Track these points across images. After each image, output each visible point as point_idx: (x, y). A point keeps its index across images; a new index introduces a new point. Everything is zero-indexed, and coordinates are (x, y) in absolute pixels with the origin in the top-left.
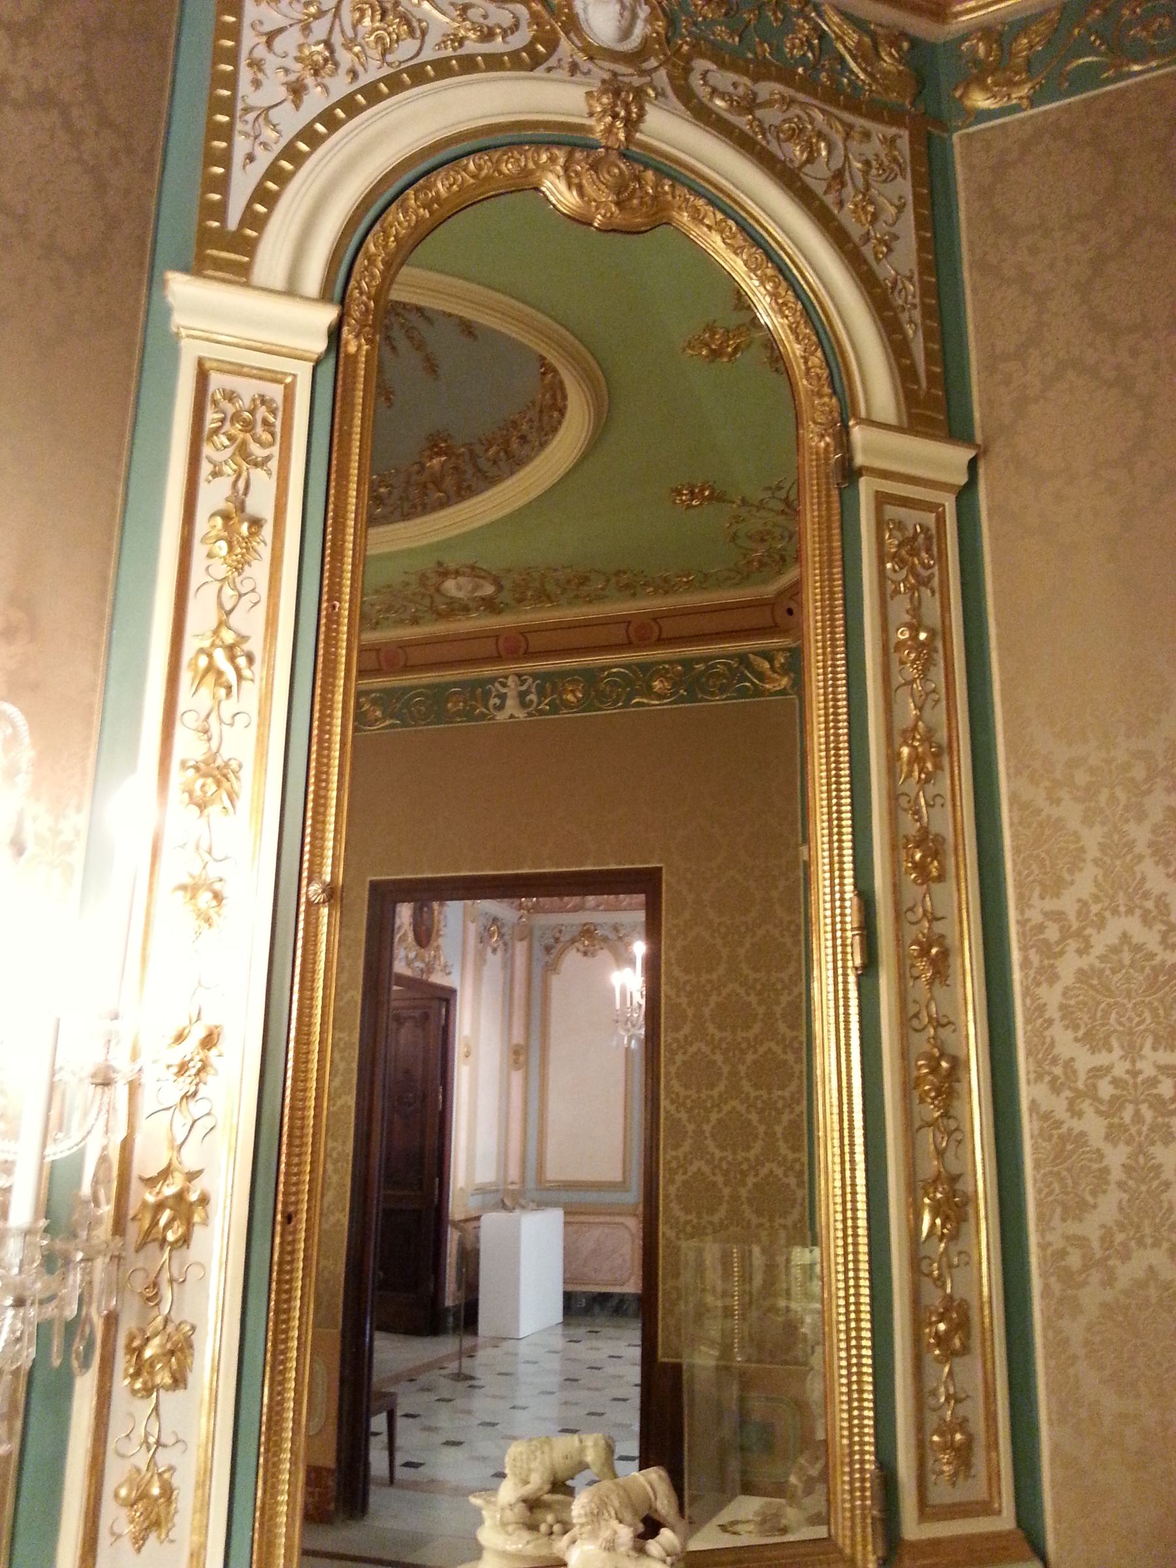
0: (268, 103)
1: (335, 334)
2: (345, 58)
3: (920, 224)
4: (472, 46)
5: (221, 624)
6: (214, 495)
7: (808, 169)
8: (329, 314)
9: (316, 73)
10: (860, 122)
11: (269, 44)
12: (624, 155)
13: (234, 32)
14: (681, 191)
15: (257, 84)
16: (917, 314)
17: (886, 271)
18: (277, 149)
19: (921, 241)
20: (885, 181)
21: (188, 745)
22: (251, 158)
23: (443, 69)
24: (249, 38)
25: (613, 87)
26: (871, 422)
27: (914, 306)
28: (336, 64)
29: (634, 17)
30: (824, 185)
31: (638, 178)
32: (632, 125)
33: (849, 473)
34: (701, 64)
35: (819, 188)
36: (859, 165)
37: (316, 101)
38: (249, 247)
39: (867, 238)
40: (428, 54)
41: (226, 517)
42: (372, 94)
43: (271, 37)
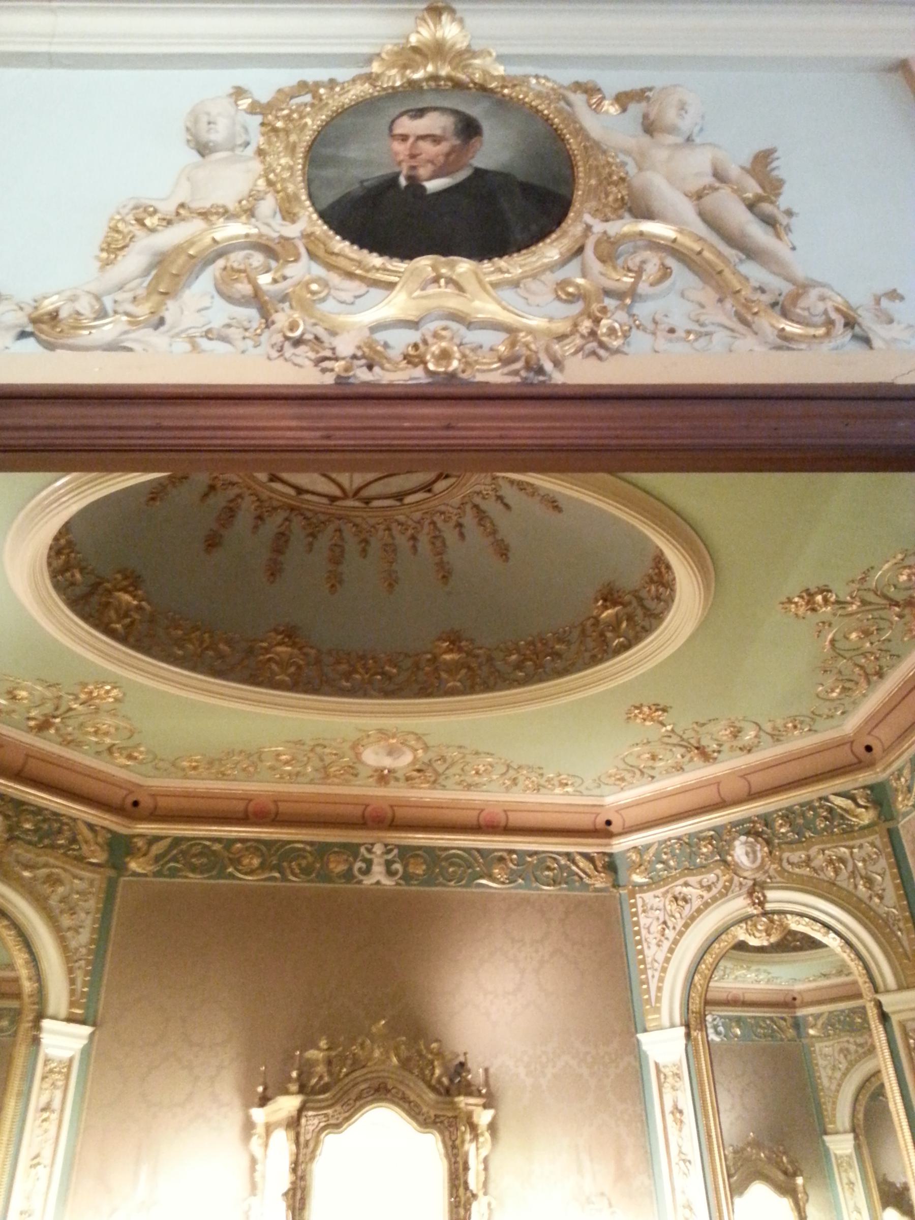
0: (653, 952)
1: (688, 1035)
2: (670, 924)
3: (894, 879)
4: (707, 895)
5: (681, 1152)
6: (668, 1107)
7: (838, 878)
8: (682, 1030)
9: (663, 935)
10: (857, 842)
11: (649, 932)
12: (765, 914)
13: (638, 933)
14: (789, 916)
15: (649, 947)
16: (901, 925)
17: (882, 910)
18: (659, 969)
19: (897, 887)
20: (874, 864)
21: (681, 1200)
22: (653, 976)
23: (699, 911)
24: (644, 932)
25: (750, 894)
26: (887, 991)
27: (899, 920)
28: (668, 927)
29: (754, 852)
30: (846, 882)
31: (772, 921)
32: (761, 904)
33: (884, 1017)
34: (786, 855)
35: (844, 884)
36: (860, 864)
37: (666, 945)
38: (657, 1010)
39: (870, 898)
40: (695, 907)
41: (672, 1113)
42: (681, 934)
43: (648, 928)
